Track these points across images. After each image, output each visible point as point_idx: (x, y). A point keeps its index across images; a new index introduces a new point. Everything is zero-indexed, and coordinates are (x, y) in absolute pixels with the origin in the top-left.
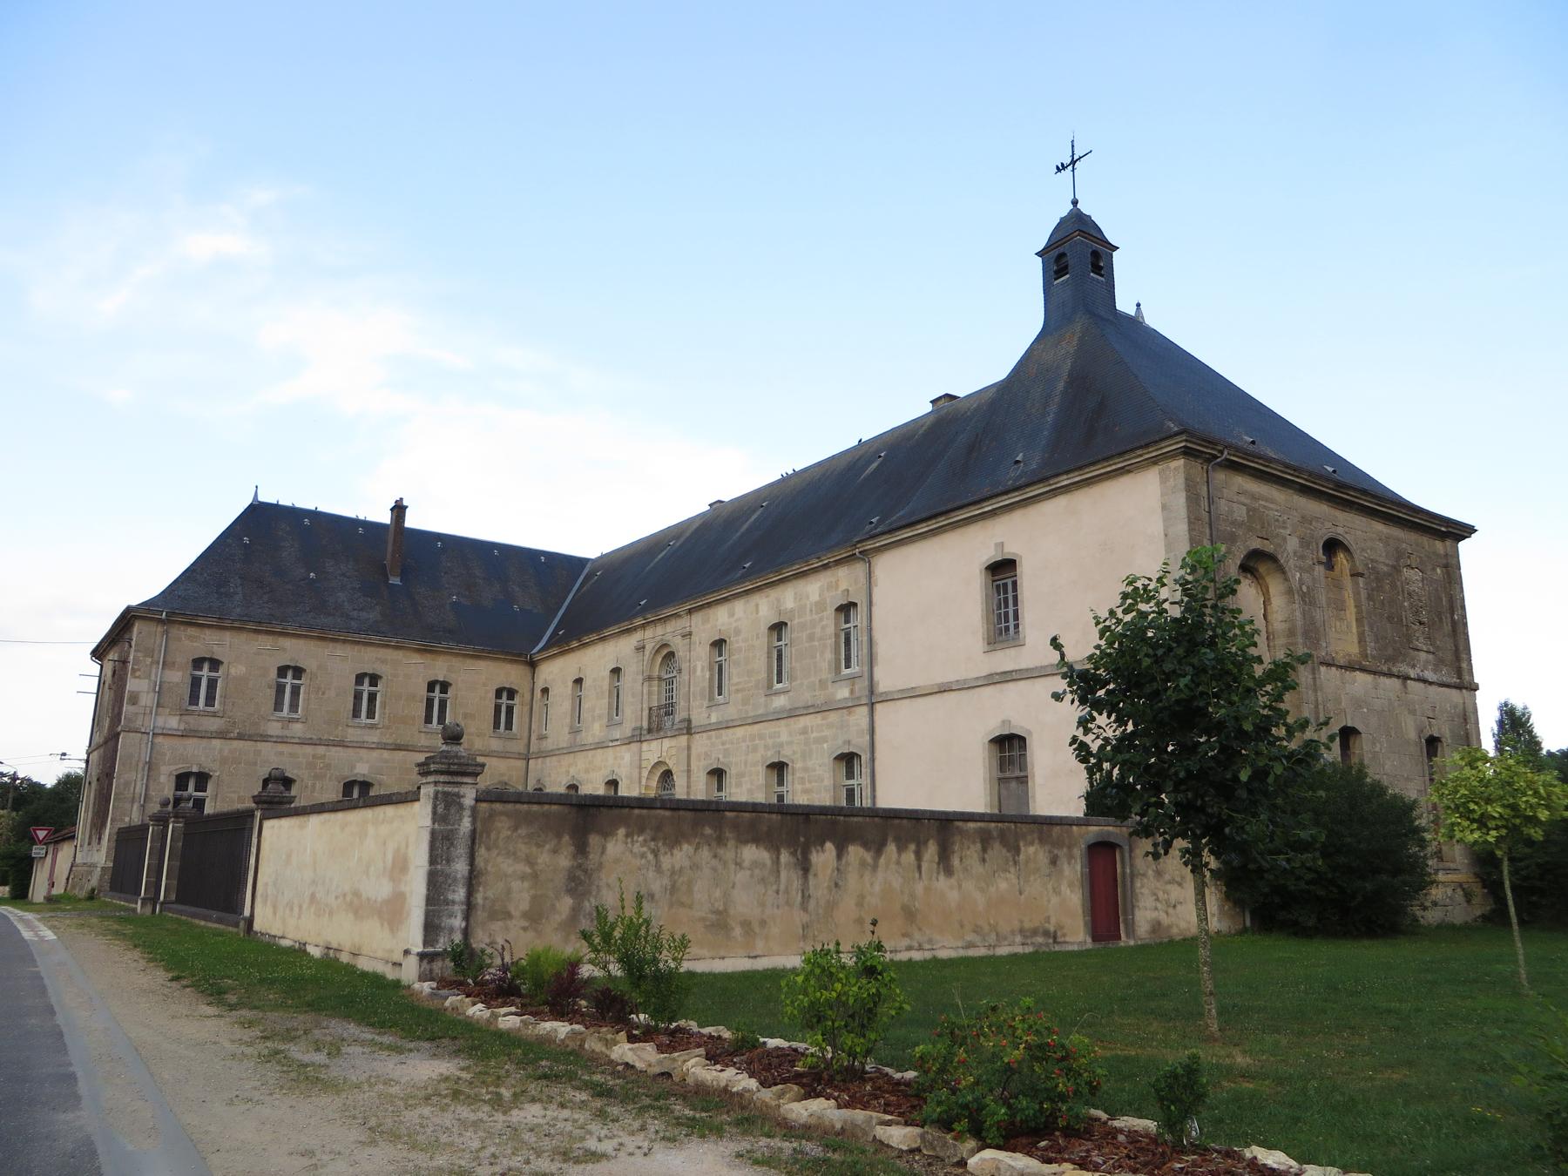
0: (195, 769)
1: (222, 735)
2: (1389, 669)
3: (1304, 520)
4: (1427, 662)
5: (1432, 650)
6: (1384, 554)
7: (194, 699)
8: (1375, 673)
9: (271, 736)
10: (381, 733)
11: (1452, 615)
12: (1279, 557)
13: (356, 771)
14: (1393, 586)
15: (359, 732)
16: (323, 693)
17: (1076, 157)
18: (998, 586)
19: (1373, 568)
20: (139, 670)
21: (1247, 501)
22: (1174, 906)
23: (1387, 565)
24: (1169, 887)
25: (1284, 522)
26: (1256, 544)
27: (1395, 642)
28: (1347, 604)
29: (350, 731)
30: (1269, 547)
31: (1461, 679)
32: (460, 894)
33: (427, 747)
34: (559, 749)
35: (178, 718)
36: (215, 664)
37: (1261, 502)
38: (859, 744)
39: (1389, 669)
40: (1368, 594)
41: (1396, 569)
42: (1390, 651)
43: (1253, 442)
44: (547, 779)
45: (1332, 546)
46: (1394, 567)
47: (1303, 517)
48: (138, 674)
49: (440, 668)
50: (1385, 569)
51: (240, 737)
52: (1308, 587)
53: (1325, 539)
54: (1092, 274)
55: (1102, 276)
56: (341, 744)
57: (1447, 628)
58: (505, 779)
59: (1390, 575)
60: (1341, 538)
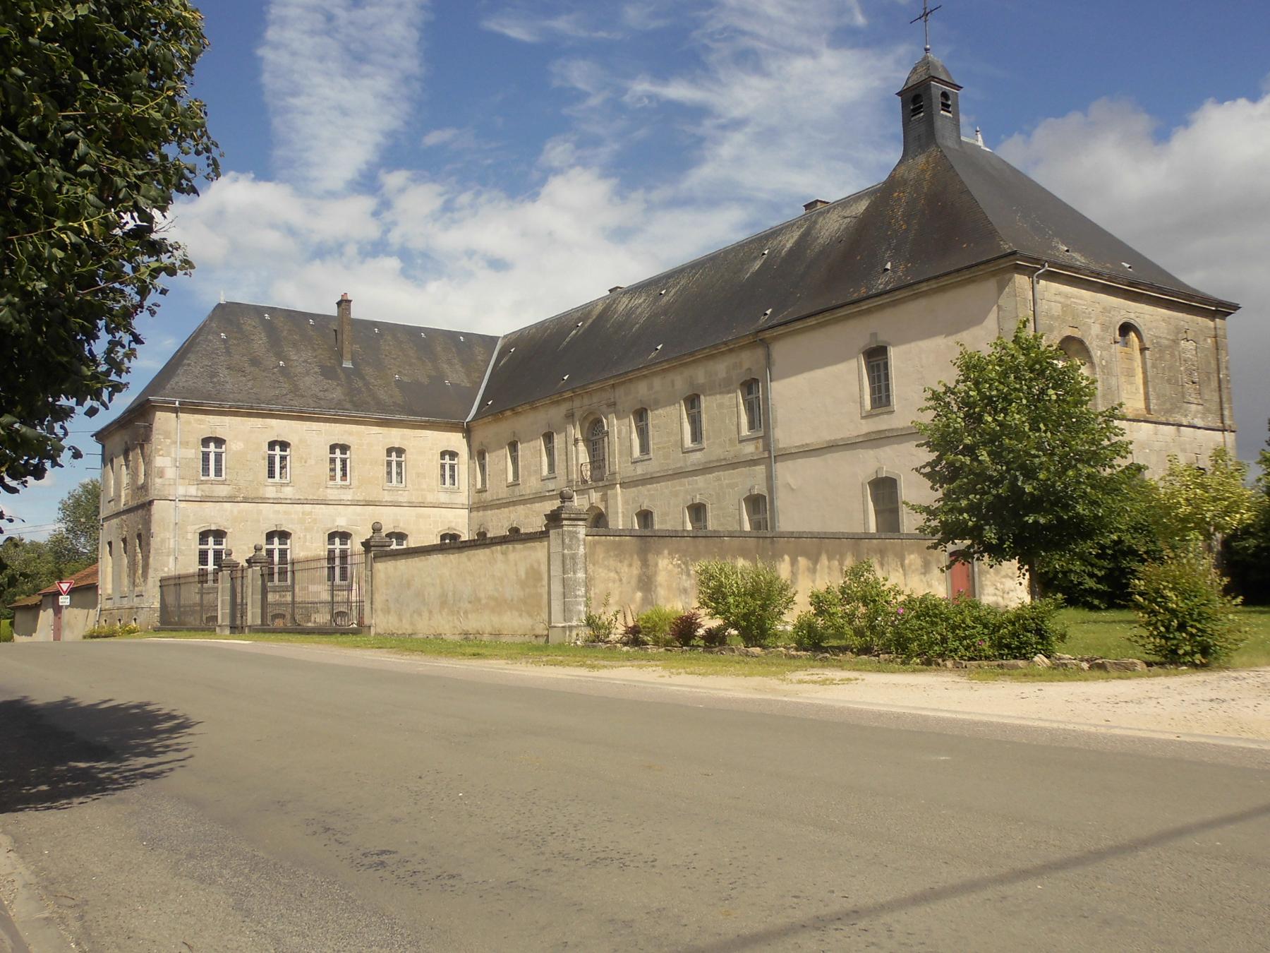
0: (213, 528)
1: (231, 500)
2: (1167, 420)
3: (1106, 310)
4: (1197, 412)
5: (1201, 402)
6: (1166, 331)
7: (206, 470)
8: (1155, 423)
9: (269, 499)
10: (354, 492)
11: (1219, 373)
12: (1085, 341)
13: (337, 524)
14: (1172, 355)
15: (336, 492)
16: (305, 462)
17: (928, 11)
18: (873, 366)
19: (1157, 343)
20: (161, 449)
21: (1062, 300)
22: (1008, 593)
23: (1168, 339)
24: (1004, 580)
25: (1090, 313)
26: (1068, 332)
27: (1172, 398)
28: (1137, 371)
29: (329, 491)
30: (1077, 334)
31: (1222, 423)
32: (582, 591)
33: (390, 502)
34: (498, 500)
35: (196, 486)
36: (219, 442)
37: (1072, 300)
38: (761, 488)
39: (1167, 420)
40: (1153, 364)
41: (1175, 342)
42: (1168, 406)
43: (1067, 251)
44: (490, 524)
45: (1126, 329)
46: (1173, 341)
47: (1104, 309)
48: (161, 453)
49: (396, 436)
50: (1166, 342)
51: (245, 501)
52: (1107, 362)
53: (1120, 323)
54: (942, 112)
55: (950, 112)
56: (325, 503)
57: (1214, 384)
58: (453, 525)
59: (1170, 347)
60: (1132, 322)
